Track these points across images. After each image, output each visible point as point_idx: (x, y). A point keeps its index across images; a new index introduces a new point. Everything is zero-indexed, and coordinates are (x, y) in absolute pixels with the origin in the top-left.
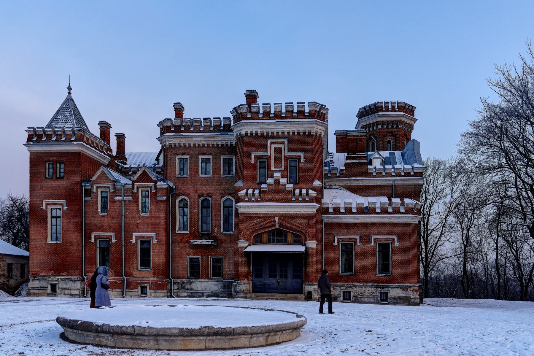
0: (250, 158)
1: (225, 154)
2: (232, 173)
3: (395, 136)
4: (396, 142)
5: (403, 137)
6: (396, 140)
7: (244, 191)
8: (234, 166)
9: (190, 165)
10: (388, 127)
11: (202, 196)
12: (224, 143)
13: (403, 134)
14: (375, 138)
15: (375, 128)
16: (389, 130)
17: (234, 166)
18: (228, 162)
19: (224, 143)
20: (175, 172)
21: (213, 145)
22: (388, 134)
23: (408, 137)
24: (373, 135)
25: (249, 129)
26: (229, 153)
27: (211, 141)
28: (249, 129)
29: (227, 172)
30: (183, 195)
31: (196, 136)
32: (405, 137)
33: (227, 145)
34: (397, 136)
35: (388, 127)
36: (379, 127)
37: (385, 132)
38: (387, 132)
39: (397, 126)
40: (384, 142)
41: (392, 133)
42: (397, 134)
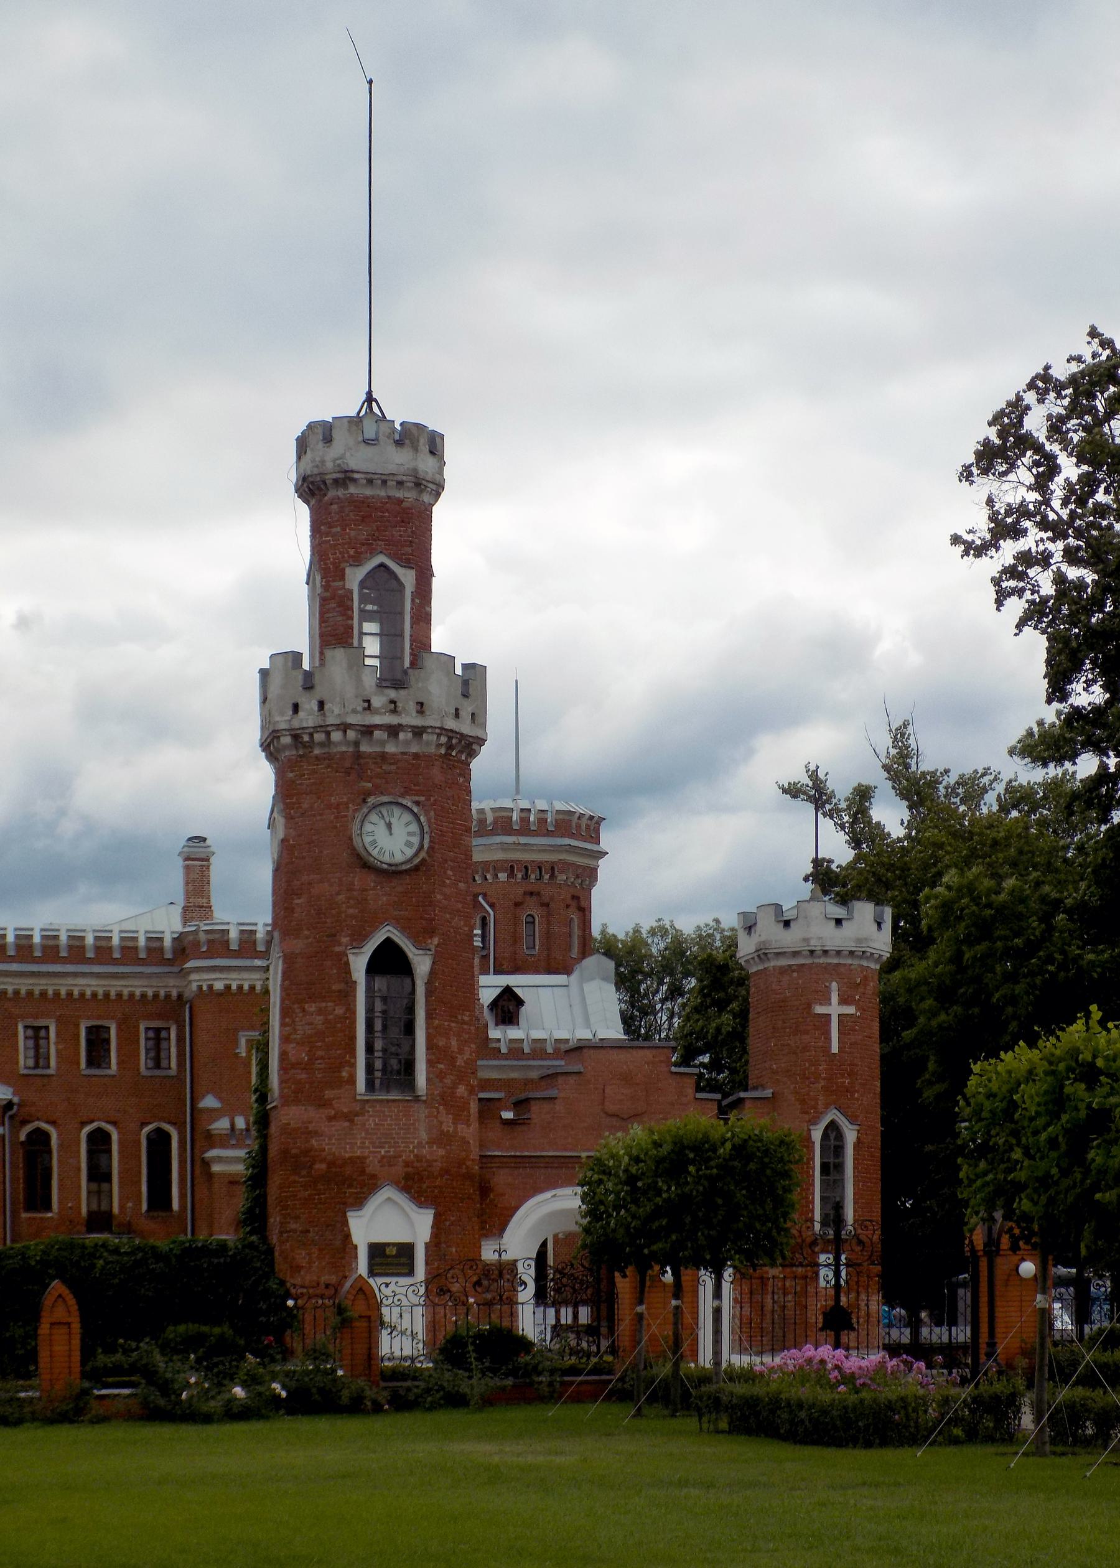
0: (236, 1043)
1: (149, 1017)
2: (164, 1063)
3: (547, 905)
4: (549, 923)
5: (568, 906)
6: (549, 914)
7: (223, 1124)
8: (173, 1050)
9: (56, 1043)
10: (526, 876)
11: (92, 1121)
12: (150, 993)
13: (569, 896)
14: (492, 906)
15: (488, 876)
16: (530, 888)
17: (173, 1050)
18: (158, 1038)
19: (150, 993)
20: (17, 1063)
21: (119, 995)
22: (528, 898)
23: (583, 904)
24: (485, 896)
25: (234, 980)
26: (160, 1016)
27: (115, 987)
28: (234, 980)
29: (151, 1064)
30: (38, 1119)
31: (75, 975)
32: (574, 904)
33: (156, 996)
34: (552, 905)
35: (526, 876)
36: (503, 876)
37: (521, 891)
38: (525, 893)
39: (552, 876)
40: (516, 922)
41: (538, 894)
42: (552, 898)
